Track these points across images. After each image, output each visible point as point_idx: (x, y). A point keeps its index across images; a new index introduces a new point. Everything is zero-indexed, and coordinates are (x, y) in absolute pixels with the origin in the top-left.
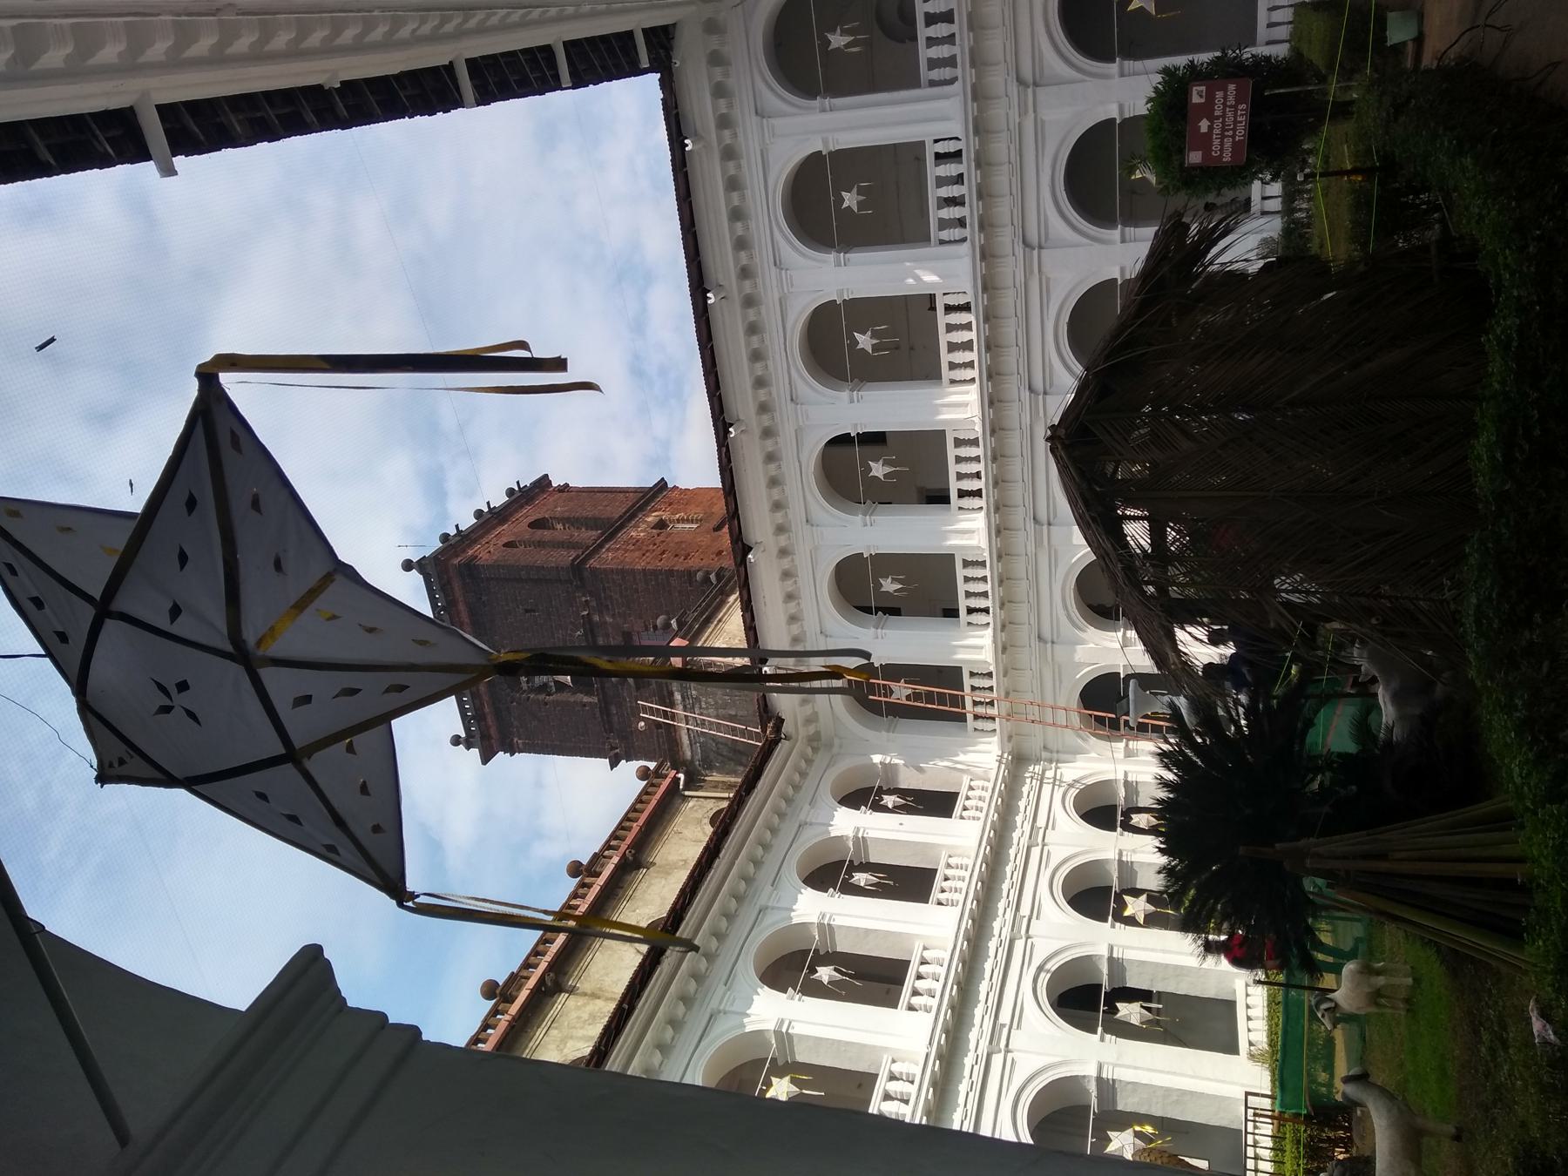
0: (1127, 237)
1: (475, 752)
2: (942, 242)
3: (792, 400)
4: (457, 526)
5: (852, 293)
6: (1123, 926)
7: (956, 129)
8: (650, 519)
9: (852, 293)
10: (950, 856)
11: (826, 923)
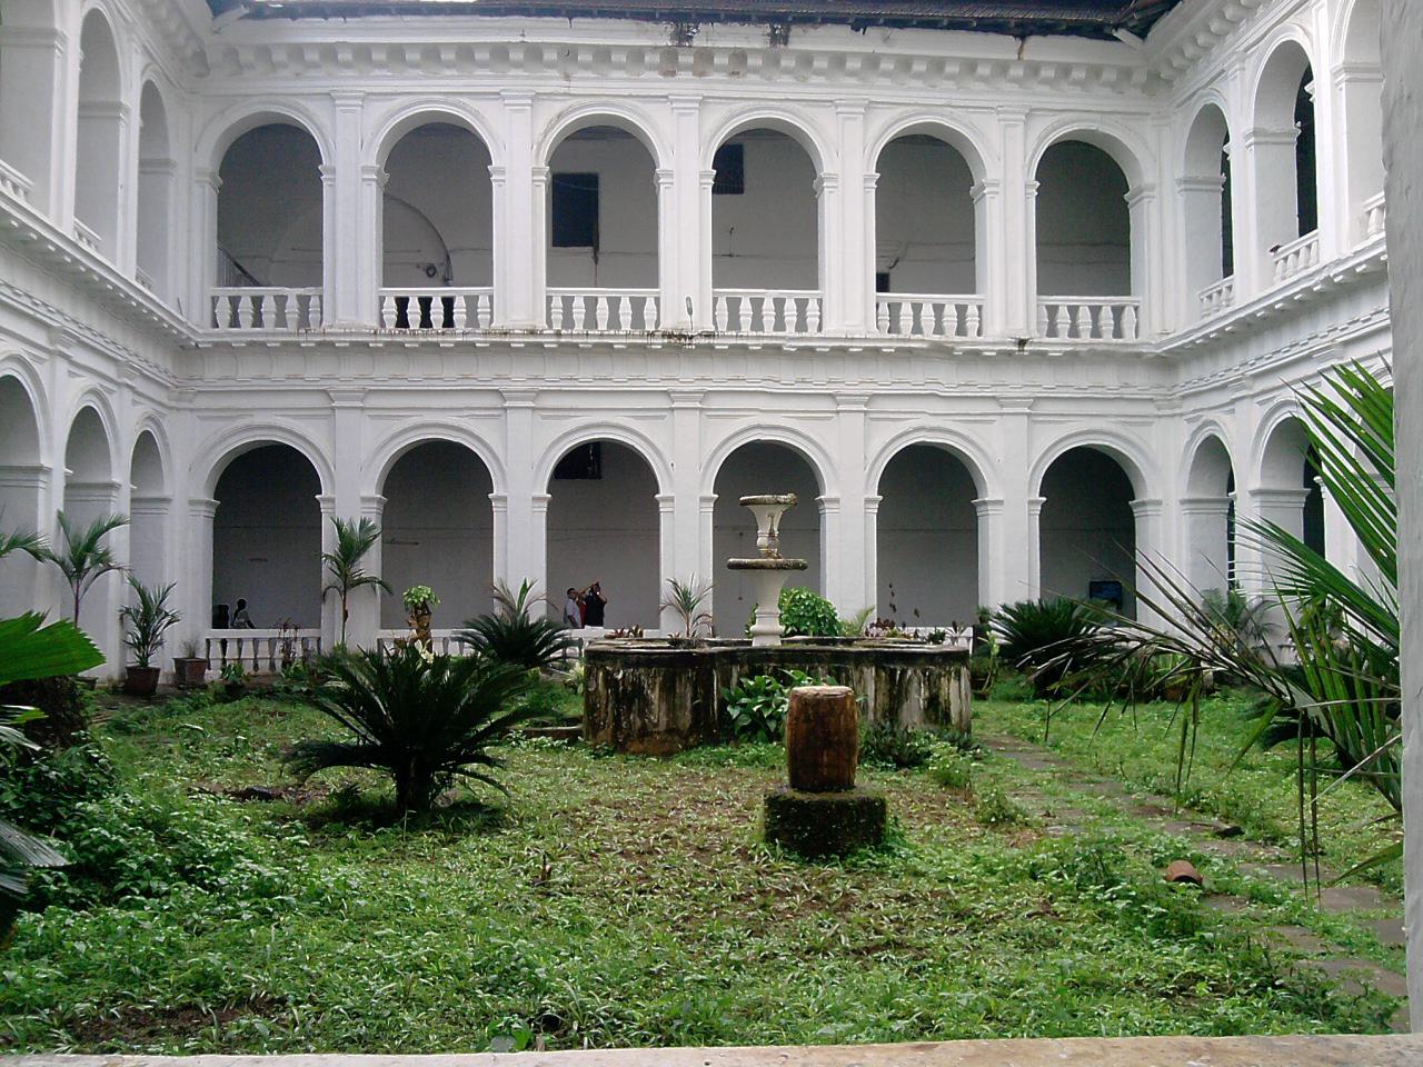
2: (549, 299)
5: (993, 198)
7: (831, 328)
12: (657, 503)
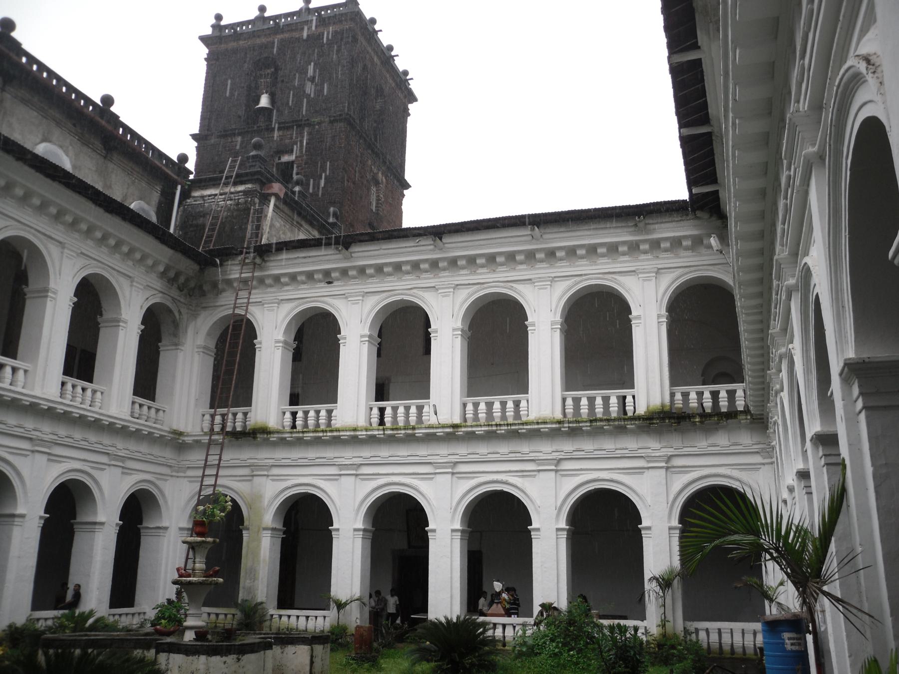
0: (560, 533)
1: (209, 31)
3: (457, 285)
4: (381, 31)
6: (41, 525)
8: (380, 175)
9: (532, 333)
10: (102, 393)
11: (50, 294)
12: (427, 532)
